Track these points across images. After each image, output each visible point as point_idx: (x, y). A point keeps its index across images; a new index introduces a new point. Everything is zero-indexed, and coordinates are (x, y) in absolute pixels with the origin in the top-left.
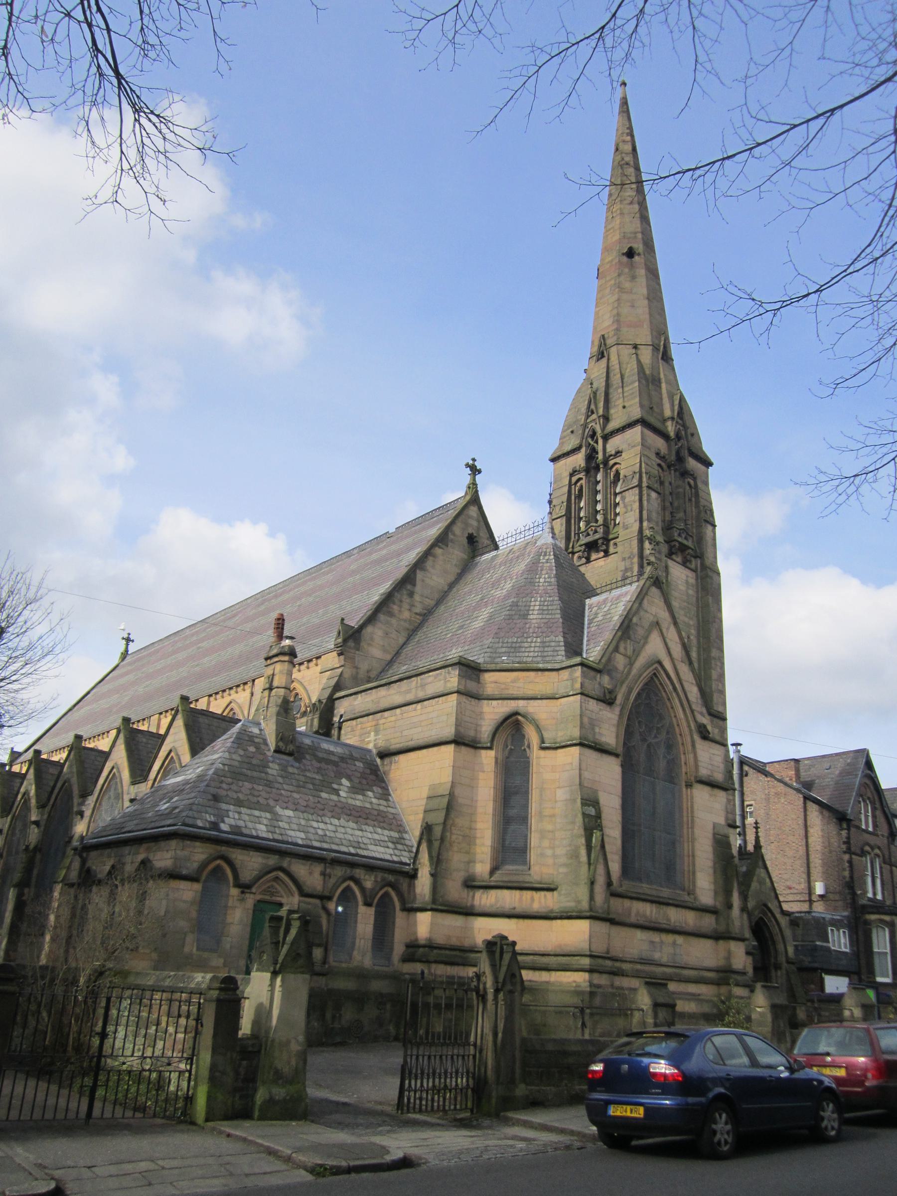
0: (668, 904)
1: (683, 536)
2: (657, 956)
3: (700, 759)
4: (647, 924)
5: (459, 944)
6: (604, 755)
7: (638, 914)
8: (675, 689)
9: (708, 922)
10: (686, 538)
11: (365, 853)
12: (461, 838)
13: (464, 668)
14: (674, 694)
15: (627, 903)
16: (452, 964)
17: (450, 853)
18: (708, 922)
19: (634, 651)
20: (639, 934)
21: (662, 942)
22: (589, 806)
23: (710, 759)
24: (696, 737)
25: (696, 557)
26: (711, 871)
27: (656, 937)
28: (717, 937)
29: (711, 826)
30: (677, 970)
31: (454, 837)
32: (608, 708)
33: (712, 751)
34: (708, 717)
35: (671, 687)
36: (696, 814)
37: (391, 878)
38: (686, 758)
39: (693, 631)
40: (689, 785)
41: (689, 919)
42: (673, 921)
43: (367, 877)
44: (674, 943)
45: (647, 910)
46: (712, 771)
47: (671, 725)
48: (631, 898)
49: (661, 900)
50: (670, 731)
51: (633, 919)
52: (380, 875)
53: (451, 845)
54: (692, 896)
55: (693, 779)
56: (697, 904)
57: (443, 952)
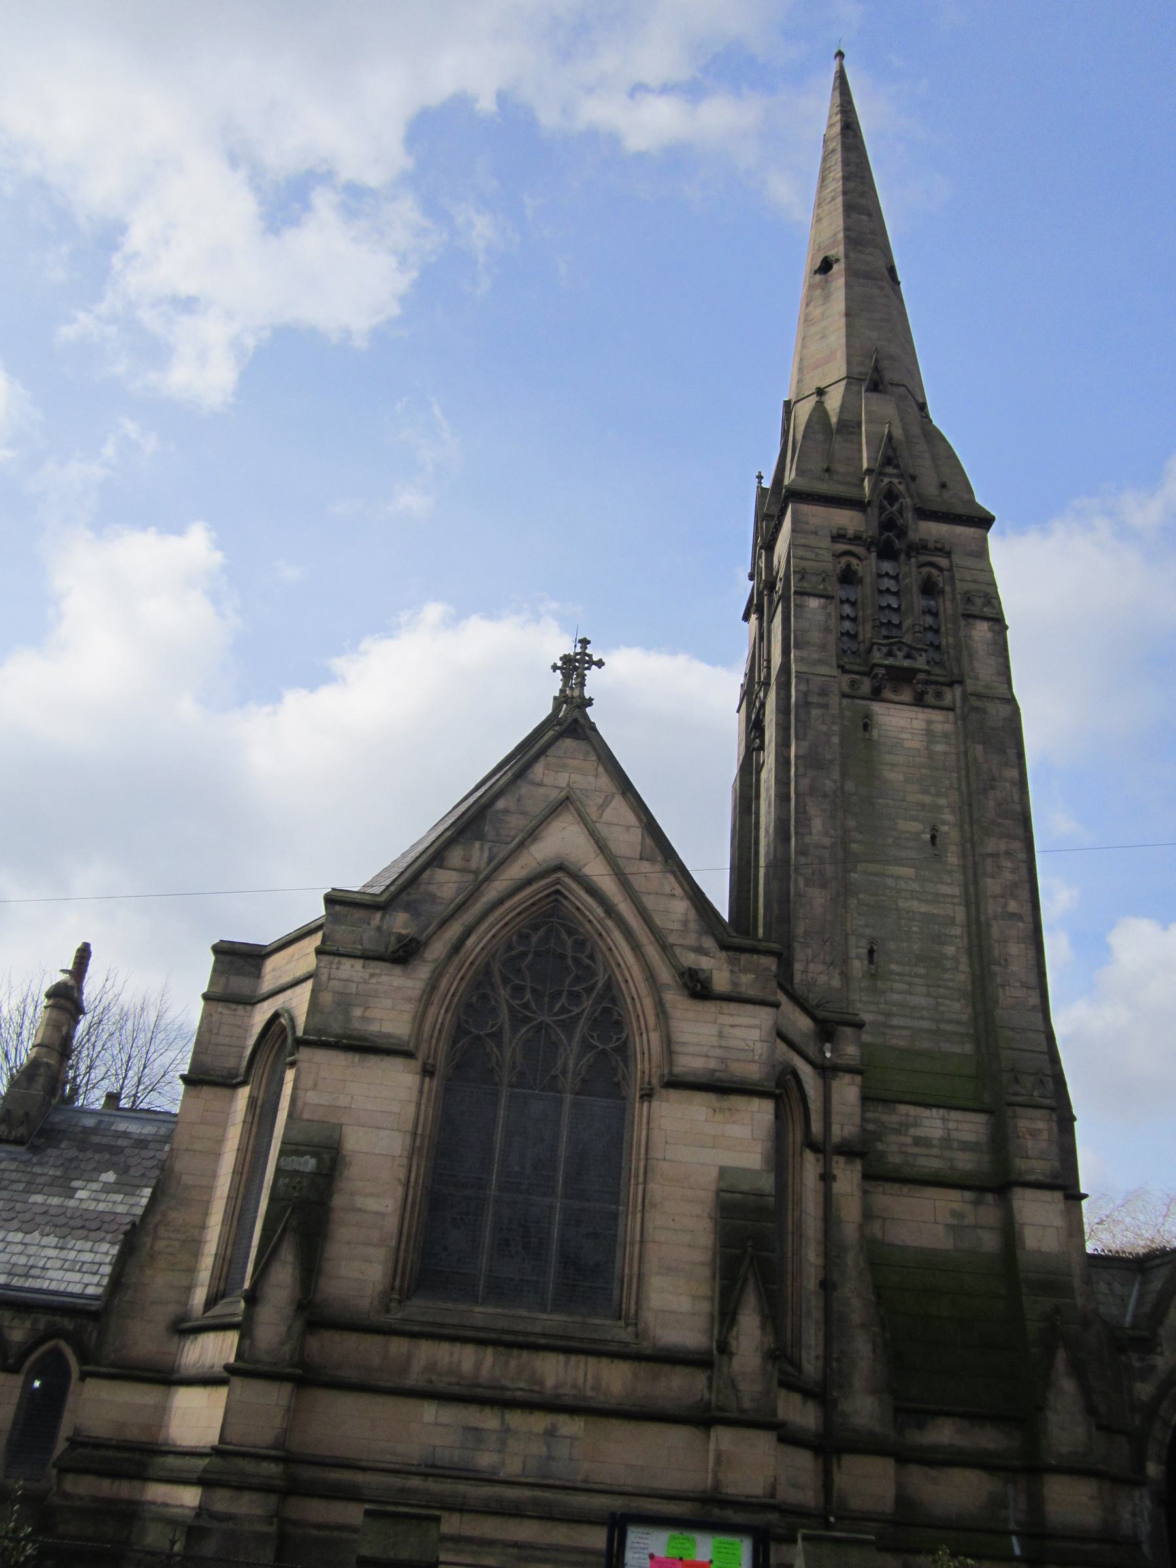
0: (535, 1347)
1: (900, 654)
2: (485, 1460)
3: (678, 1036)
4: (456, 1390)
5: (143, 1439)
6: (373, 1061)
7: (431, 1367)
8: (610, 910)
9: (681, 1386)
10: (908, 656)
11: (45, 1285)
12: (177, 1244)
13: (229, 958)
14: (609, 923)
15: (398, 1346)
16: (115, 1475)
17: (149, 1272)
18: (681, 1386)
19: (490, 859)
20: (429, 1412)
21: (507, 1430)
22: (303, 1154)
23: (720, 1035)
24: (675, 999)
25: (951, 685)
26: (706, 1272)
27: (489, 1420)
28: (702, 1419)
29: (714, 1173)
30: (538, 1493)
31: (161, 1244)
32: (398, 970)
33: (726, 1020)
34: (723, 955)
35: (600, 911)
36: (656, 1154)
37: (68, 1324)
38: (647, 1045)
39: (948, 817)
40: (647, 1095)
41: (616, 1380)
42: (550, 1383)
43: (16, 1322)
44: (551, 1433)
45: (466, 1360)
46: (723, 1060)
47: (609, 985)
48: (413, 1335)
49: (572, 1344)
50: (611, 993)
51: (414, 1379)
52: (43, 1321)
53: (152, 1257)
54: (631, 1329)
55: (655, 1081)
56: (646, 1347)
57: (102, 1452)
